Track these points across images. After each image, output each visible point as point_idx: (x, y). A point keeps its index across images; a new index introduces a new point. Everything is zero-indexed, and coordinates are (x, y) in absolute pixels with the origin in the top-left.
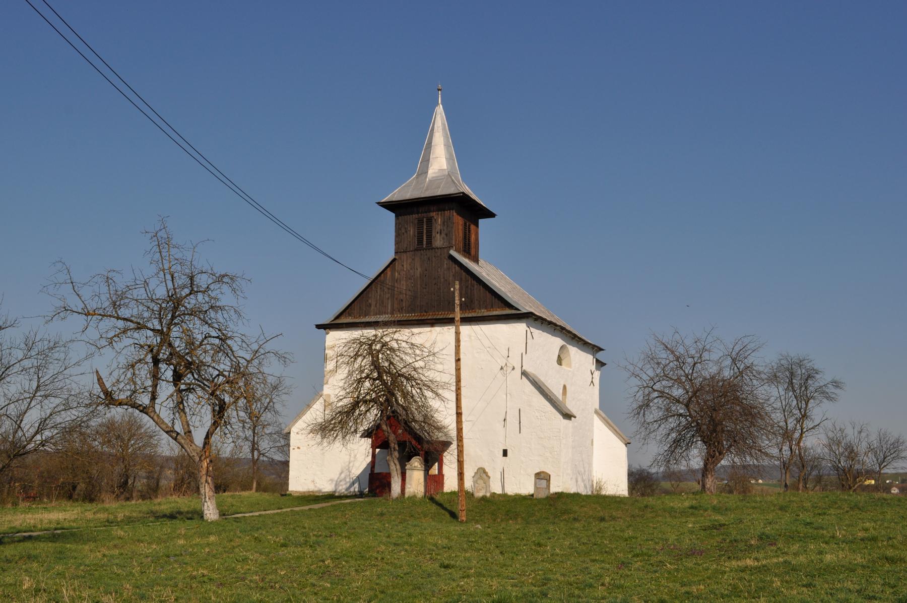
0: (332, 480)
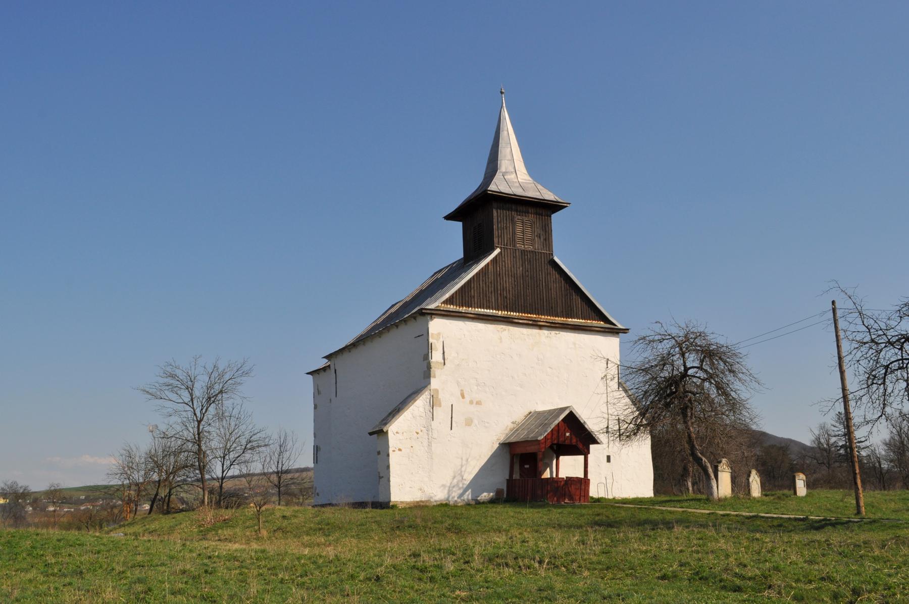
0: (444, 486)
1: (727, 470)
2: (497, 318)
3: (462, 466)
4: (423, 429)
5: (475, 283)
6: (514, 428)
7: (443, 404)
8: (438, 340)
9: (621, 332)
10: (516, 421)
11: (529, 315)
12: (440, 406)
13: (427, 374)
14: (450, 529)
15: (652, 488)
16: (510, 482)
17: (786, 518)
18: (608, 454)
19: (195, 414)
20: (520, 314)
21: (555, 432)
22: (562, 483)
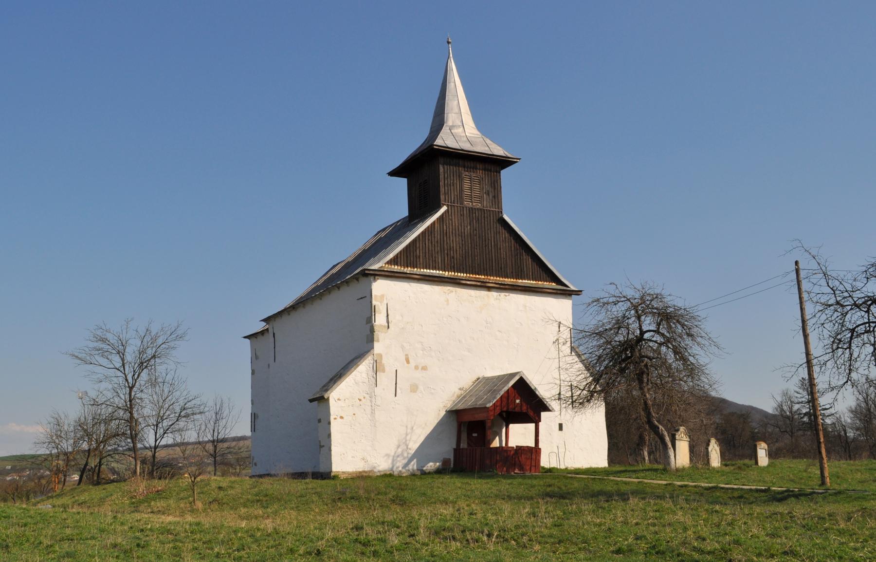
0: (388, 455)
1: (684, 439)
2: (444, 280)
3: (407, 435)
4: (365, 395)
5: (421, 243)
6: (462, 395)
7: (387, 369)
8: (381, 302)
9: (574, 293)
10: (463, 388)
11: (477, 276)
12: (384, 371)
13: (370, 338)
14: (394, 500)
15: (607, 458)
16: (457, 451)
17: (748, 489)
18: (560, 422)
19: (127, 380)
20: (468, 275)
21: (504, 399)
22: (512, 453)
